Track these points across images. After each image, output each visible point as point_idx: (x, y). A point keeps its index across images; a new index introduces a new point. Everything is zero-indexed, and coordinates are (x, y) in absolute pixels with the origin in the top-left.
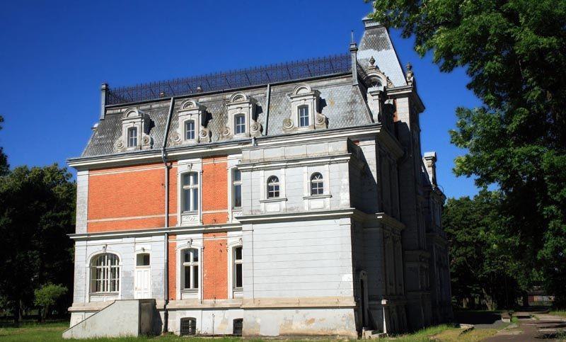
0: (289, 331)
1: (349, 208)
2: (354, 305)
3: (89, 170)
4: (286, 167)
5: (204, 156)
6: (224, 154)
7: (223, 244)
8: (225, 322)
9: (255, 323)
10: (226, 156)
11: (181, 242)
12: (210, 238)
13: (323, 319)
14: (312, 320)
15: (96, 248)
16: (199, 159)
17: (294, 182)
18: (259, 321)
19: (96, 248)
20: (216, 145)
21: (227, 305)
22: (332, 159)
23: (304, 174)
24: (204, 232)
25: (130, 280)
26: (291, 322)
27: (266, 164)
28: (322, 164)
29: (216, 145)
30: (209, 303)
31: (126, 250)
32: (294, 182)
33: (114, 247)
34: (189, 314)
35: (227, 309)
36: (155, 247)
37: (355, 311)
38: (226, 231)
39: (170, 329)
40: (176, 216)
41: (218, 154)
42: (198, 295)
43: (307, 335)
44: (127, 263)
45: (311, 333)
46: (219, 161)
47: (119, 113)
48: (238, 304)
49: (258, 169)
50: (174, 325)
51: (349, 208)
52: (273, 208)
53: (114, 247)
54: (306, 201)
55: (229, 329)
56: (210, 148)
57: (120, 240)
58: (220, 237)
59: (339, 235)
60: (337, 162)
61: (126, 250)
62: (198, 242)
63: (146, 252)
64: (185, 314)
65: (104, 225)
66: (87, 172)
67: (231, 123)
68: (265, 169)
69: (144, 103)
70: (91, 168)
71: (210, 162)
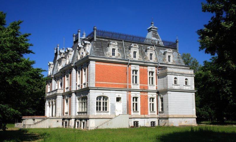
0: (181, 125)
1: (194, 90)
2: (196, 117)
3: (96, 61)
4: (180, 75)
5: (140, 65)
6: (147, 66)
7: (147, 96)
8: (148, 122)
9: (172, 122)
10: (147, 66)
11: (133, 94)
12: (143, 94)
13: (189, 121)
14: (186, 122)
15: (99, 93)
16: (138, 66)
17: (181, 80)
18: (173, 122)
19: (99, 93)
20: (147, 62)
21: (149, 117)
22: (191, 75)
23: (174, 77)
24: (141, 92)
25: (113, 107)
26: (181, 122)
27: (175, 74)
28: (188, 76)
29: (147, 62)
30: (143, 116)
31: (112, 96)
32: (181, 80)
33: (106, 93)
34: (136, 120)
35: (149, 118)
36: (123, 95)
37: (196, 120)
38: (130, 91)
39: (70, 125)
40: (140, 84)
41: (121, 63)
42: (139, 113)
43: (186, 126)
44: (112, 100)
45: (186, 125)
46: (145, 68)
47: (101, 40)
48: (152, 116)
49: (172, 75)
50: (131, 124)
51: (194, 90)
52: (176, 87)
53: (106, 93)
54: (184, 86)
55: (149, 125)
56: (145, 63)
57: (110, 91)
58: (146, 94)
59: (191, 98)
60: (192, 76)
61: (112, 96)
62: (138, 95)
63: (120, 97)
64: (135, 120)
65: (103, 85)
66: (95, 62)
67: (148, 56)
68: (174, 75)
69: (129, 42)
70: (97, 61)
71: (142, 68)
